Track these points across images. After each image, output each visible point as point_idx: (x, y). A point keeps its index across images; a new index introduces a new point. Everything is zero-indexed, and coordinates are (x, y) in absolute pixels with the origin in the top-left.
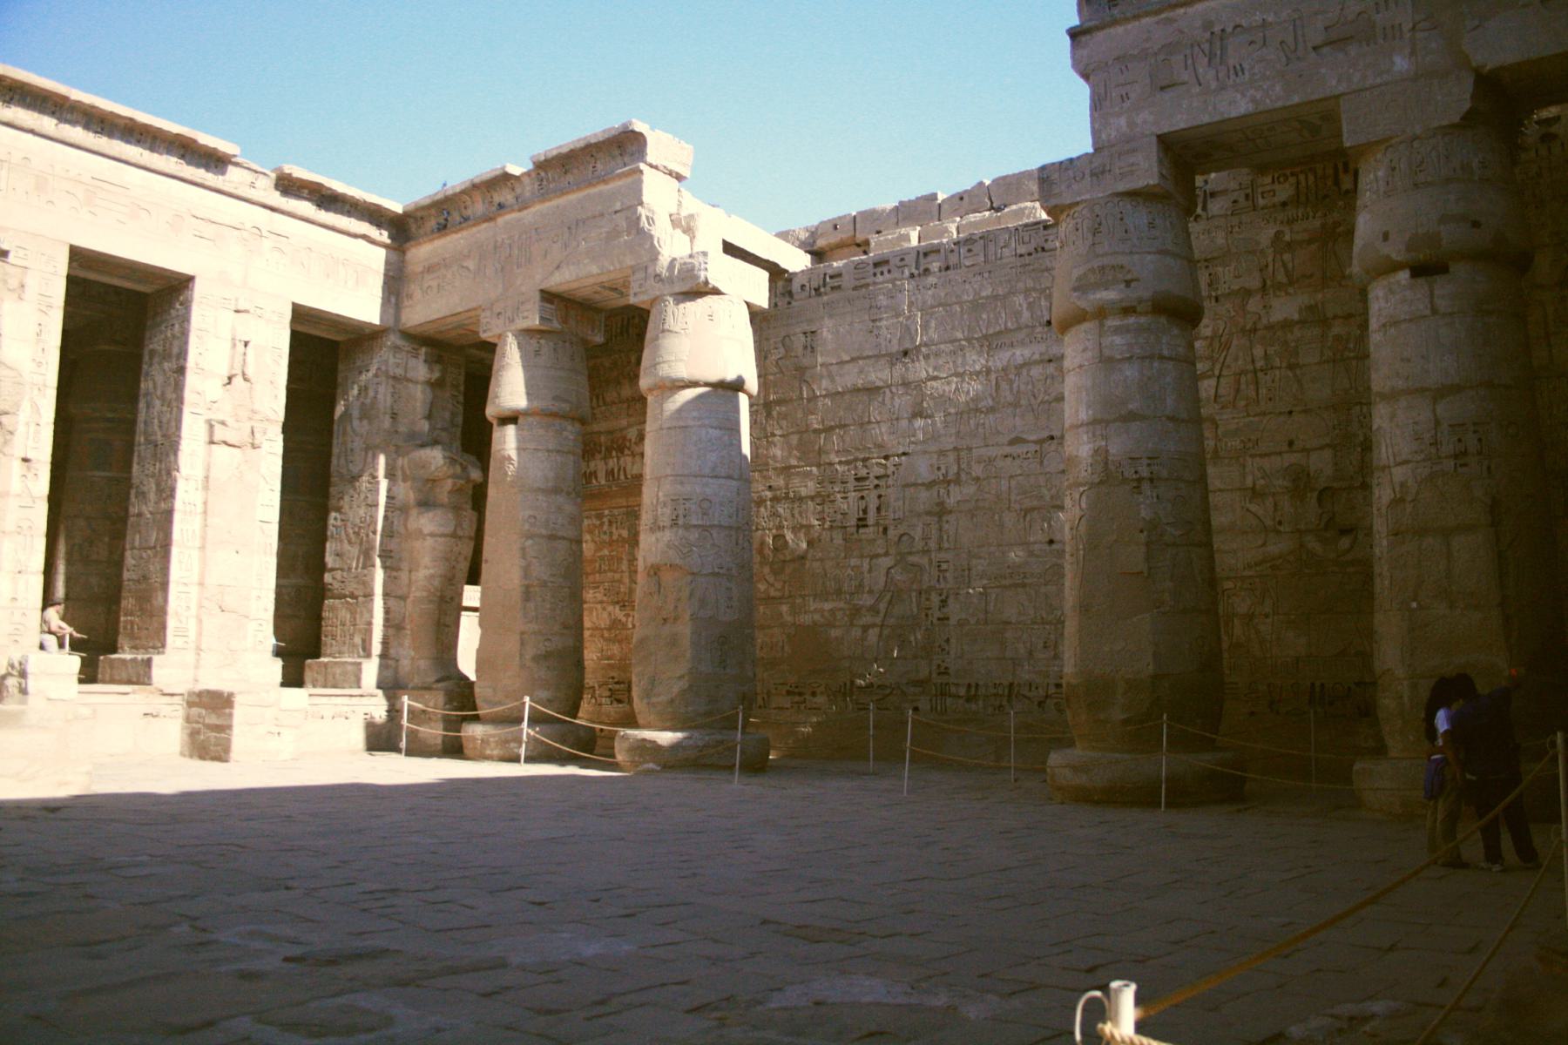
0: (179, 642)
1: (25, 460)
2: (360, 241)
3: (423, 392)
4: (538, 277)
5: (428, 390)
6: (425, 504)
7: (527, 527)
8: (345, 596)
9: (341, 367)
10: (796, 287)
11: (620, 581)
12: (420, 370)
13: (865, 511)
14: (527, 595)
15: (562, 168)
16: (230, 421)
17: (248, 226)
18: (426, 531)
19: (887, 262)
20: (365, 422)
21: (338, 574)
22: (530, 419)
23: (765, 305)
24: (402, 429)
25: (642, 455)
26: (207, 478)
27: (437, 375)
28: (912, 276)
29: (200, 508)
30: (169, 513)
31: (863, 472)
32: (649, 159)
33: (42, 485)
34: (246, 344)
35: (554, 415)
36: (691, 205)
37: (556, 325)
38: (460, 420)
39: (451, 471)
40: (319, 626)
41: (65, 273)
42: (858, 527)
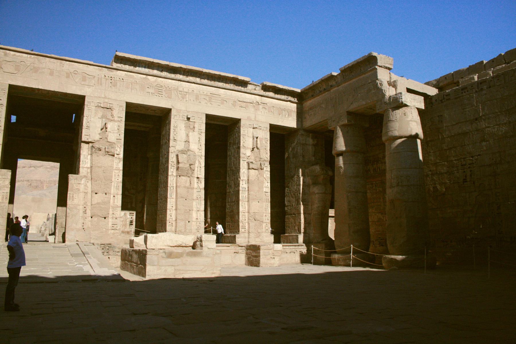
0: (243, 230)
1: (198, 178)
2: (289, 103)
6: (315, 183)
8: (291, 214)
10: (434, 100)
12: (310, 141)
13: (466, 176)
15: (349, 71)
16: (254, 162)
17: (255, 102)
19: (466, 88)
21: (289, 208)
23: (423, 108)
25: (385, 163)
26: (248, 180)
27: (316, 142)
28: (476, 92)
29: (247, 189)
30: (239, 191)
31: (464, 163)
32: (379, 64)
33: (202, 185)
34: (257, 138)
36: (394, 77)
37: (353, 122)
40: (285, 224)
41: (204, 122)
42: (464, 182)
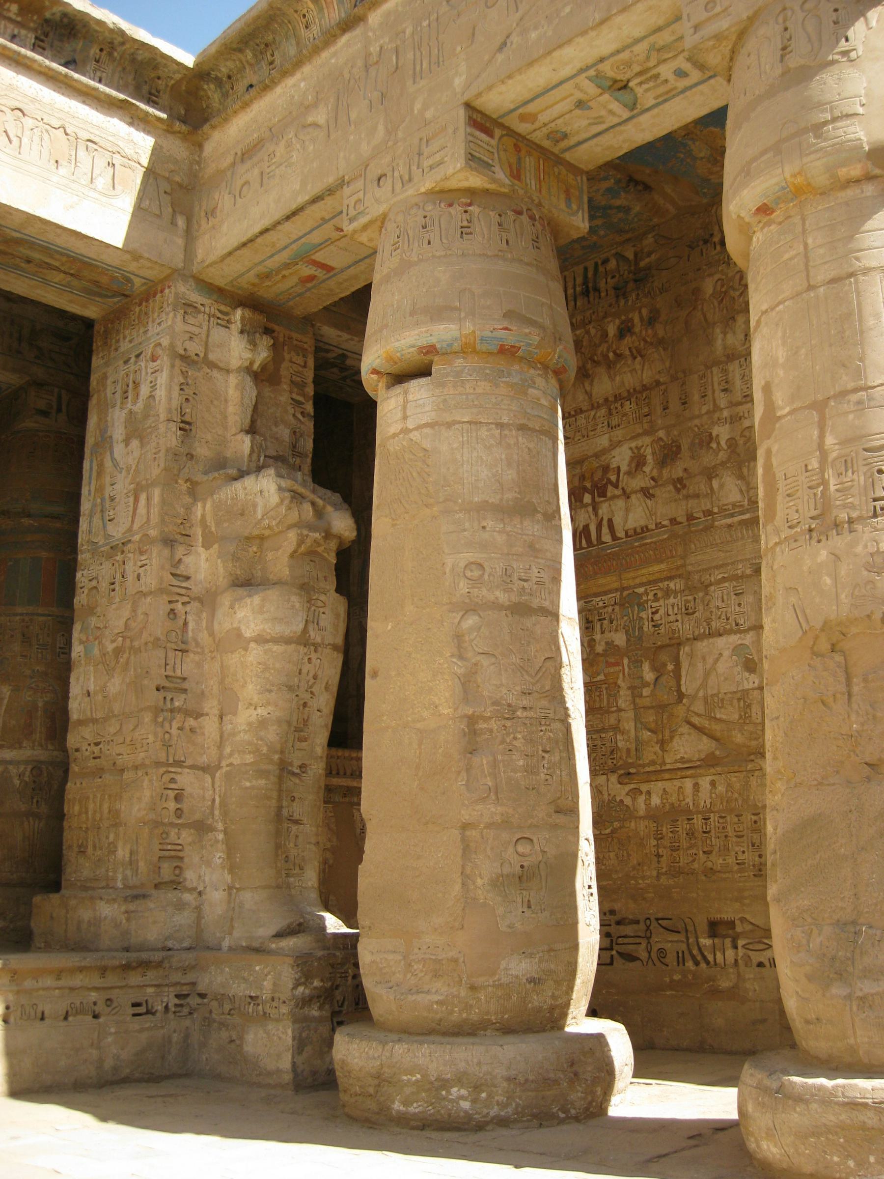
3: (241, 387)
4: (458, 82)
5: (249, 382)
6: (246, 582)
7: (463, 587)
9: (96, 361)
11: (616, 729)
12: (235, 348)
14: (472, 736)
18: (248, 634)
20: (135, 443)
22: (459, 362)
24: (202, 451)
35: (507, 352)
38: (308, 445)
39: (294, 516)
